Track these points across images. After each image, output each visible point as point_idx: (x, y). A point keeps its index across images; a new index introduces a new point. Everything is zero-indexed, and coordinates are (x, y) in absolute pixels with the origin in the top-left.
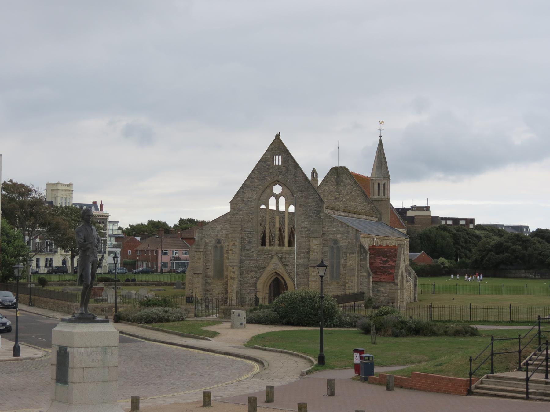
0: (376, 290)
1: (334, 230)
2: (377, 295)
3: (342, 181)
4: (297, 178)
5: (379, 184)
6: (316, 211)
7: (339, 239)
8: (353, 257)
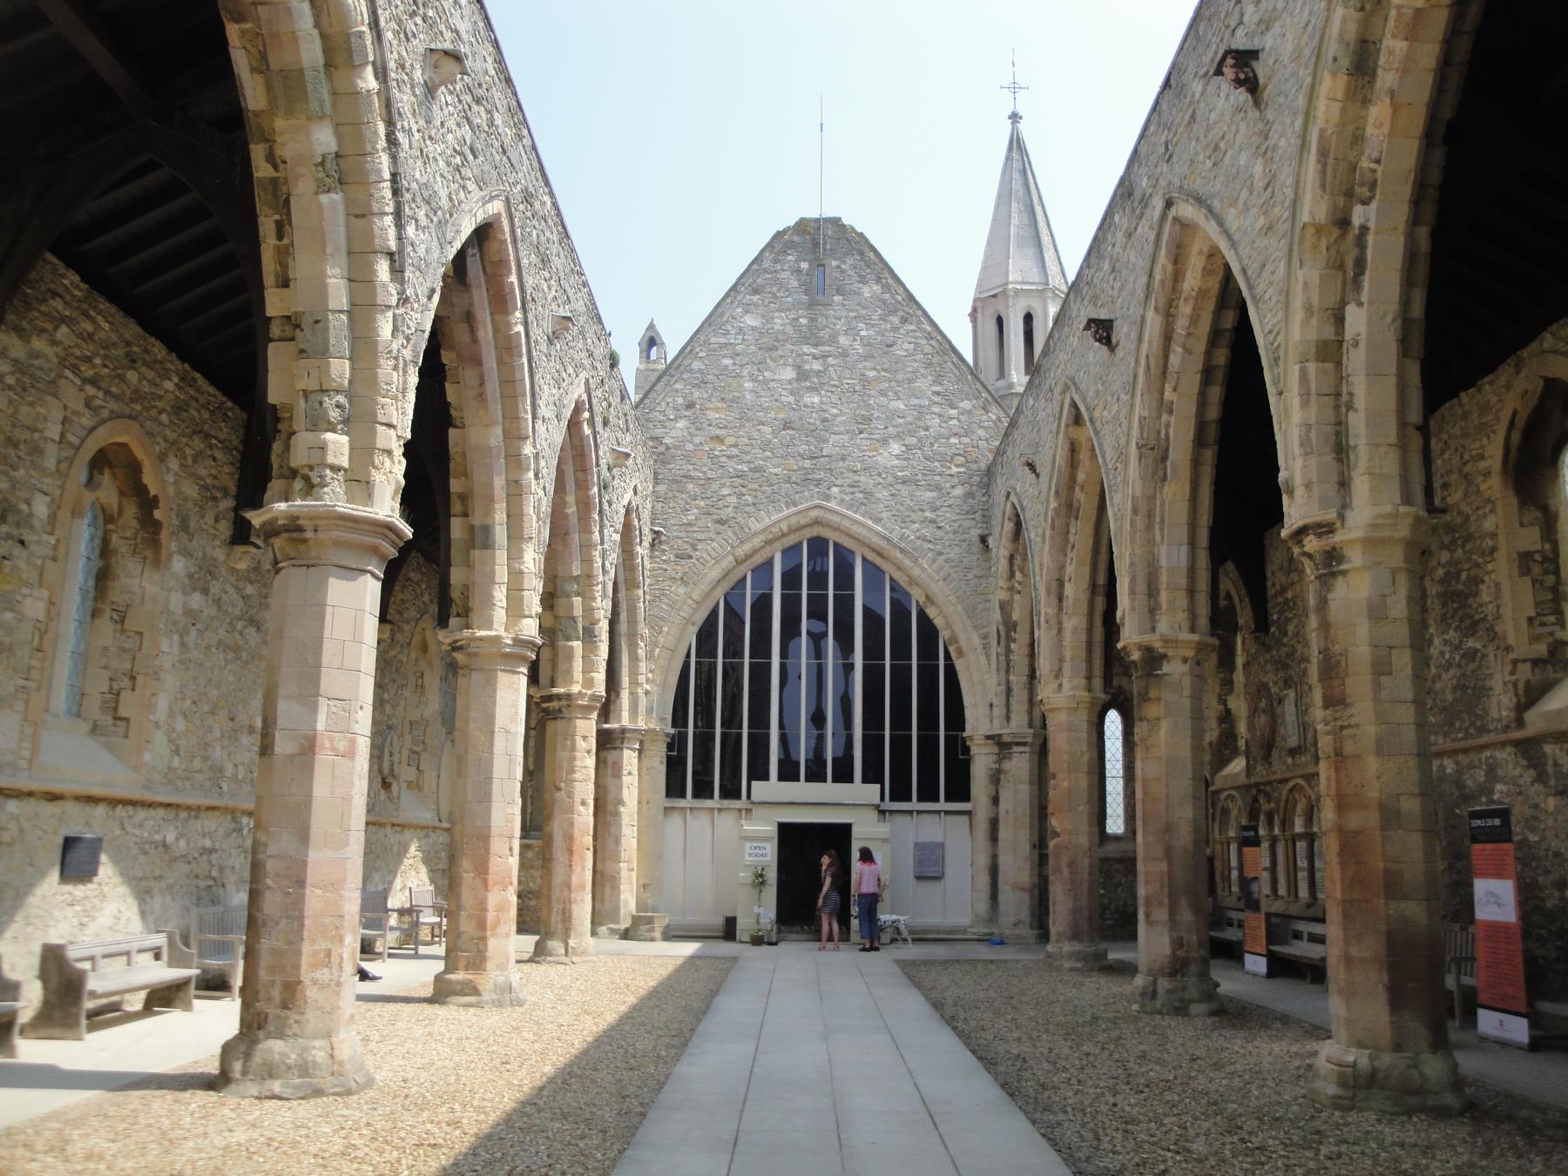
3: (839, 292)
5: (1028, 318)
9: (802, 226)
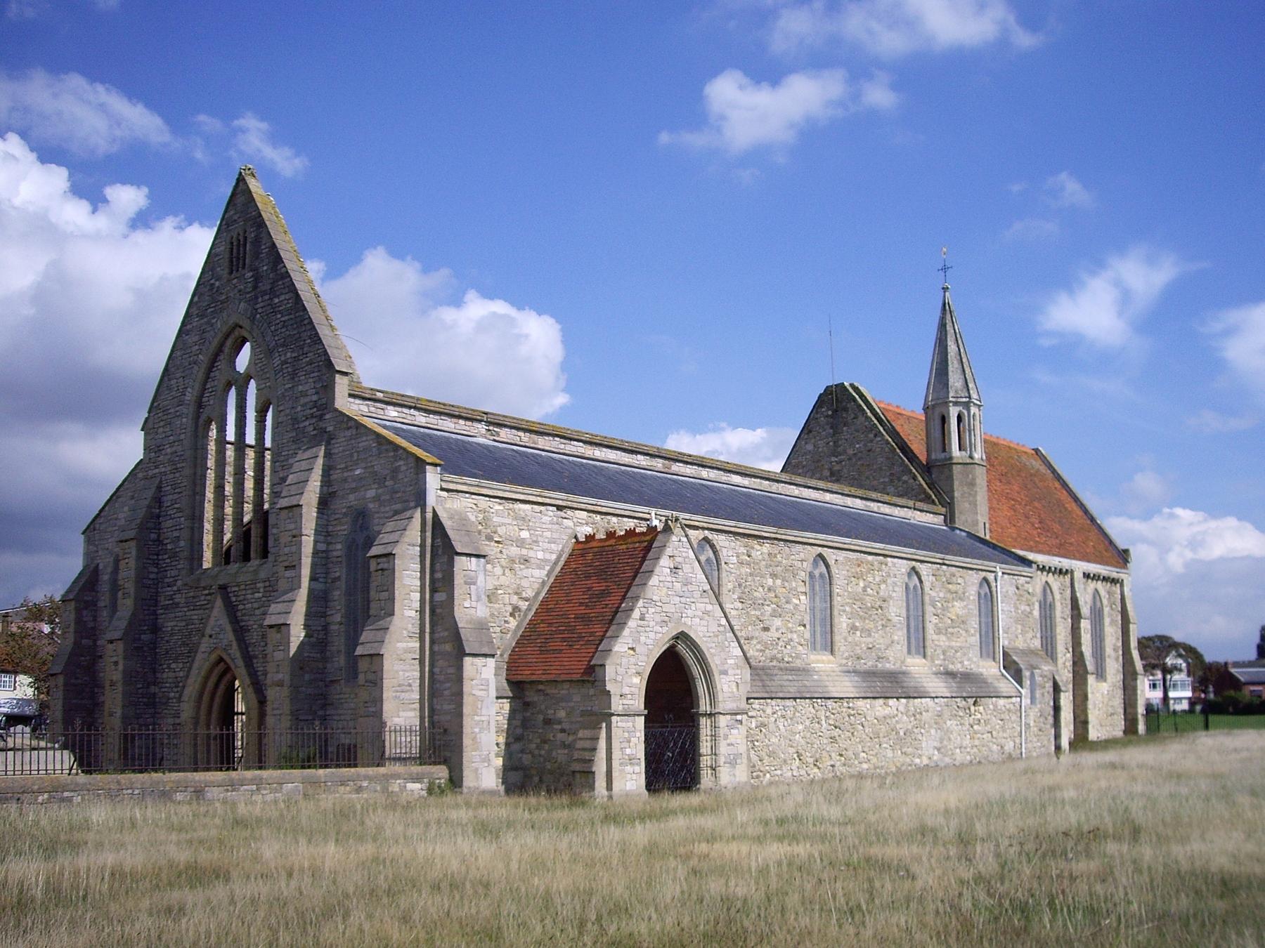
0: (541, 717)
1: (357, 472)
2: (545, 742)
4: (276, 300)
6: (315, 410)
7: (371, 506)
8: (386, 572)
9: (828, 390)
